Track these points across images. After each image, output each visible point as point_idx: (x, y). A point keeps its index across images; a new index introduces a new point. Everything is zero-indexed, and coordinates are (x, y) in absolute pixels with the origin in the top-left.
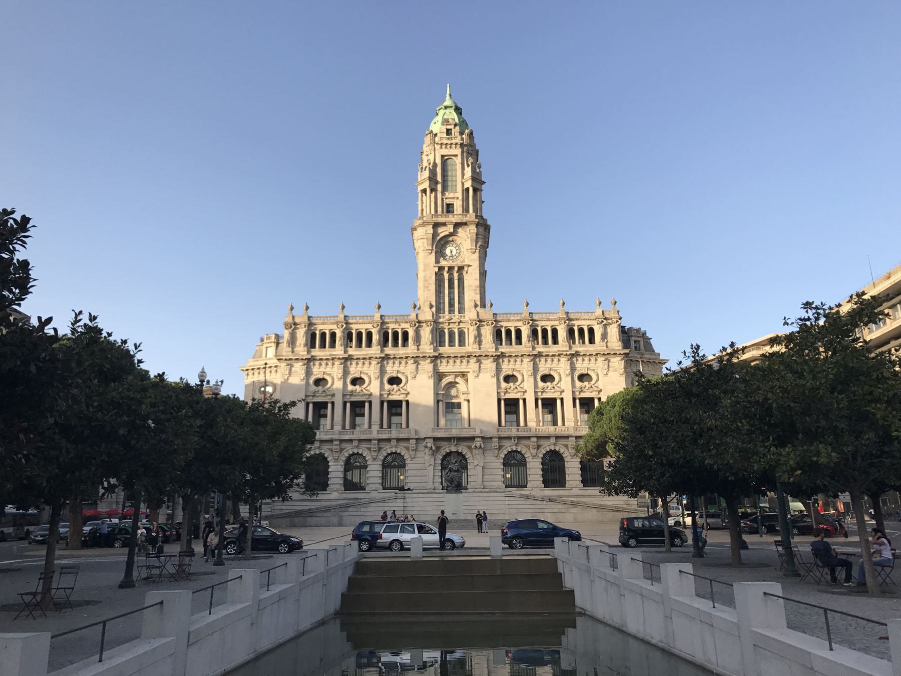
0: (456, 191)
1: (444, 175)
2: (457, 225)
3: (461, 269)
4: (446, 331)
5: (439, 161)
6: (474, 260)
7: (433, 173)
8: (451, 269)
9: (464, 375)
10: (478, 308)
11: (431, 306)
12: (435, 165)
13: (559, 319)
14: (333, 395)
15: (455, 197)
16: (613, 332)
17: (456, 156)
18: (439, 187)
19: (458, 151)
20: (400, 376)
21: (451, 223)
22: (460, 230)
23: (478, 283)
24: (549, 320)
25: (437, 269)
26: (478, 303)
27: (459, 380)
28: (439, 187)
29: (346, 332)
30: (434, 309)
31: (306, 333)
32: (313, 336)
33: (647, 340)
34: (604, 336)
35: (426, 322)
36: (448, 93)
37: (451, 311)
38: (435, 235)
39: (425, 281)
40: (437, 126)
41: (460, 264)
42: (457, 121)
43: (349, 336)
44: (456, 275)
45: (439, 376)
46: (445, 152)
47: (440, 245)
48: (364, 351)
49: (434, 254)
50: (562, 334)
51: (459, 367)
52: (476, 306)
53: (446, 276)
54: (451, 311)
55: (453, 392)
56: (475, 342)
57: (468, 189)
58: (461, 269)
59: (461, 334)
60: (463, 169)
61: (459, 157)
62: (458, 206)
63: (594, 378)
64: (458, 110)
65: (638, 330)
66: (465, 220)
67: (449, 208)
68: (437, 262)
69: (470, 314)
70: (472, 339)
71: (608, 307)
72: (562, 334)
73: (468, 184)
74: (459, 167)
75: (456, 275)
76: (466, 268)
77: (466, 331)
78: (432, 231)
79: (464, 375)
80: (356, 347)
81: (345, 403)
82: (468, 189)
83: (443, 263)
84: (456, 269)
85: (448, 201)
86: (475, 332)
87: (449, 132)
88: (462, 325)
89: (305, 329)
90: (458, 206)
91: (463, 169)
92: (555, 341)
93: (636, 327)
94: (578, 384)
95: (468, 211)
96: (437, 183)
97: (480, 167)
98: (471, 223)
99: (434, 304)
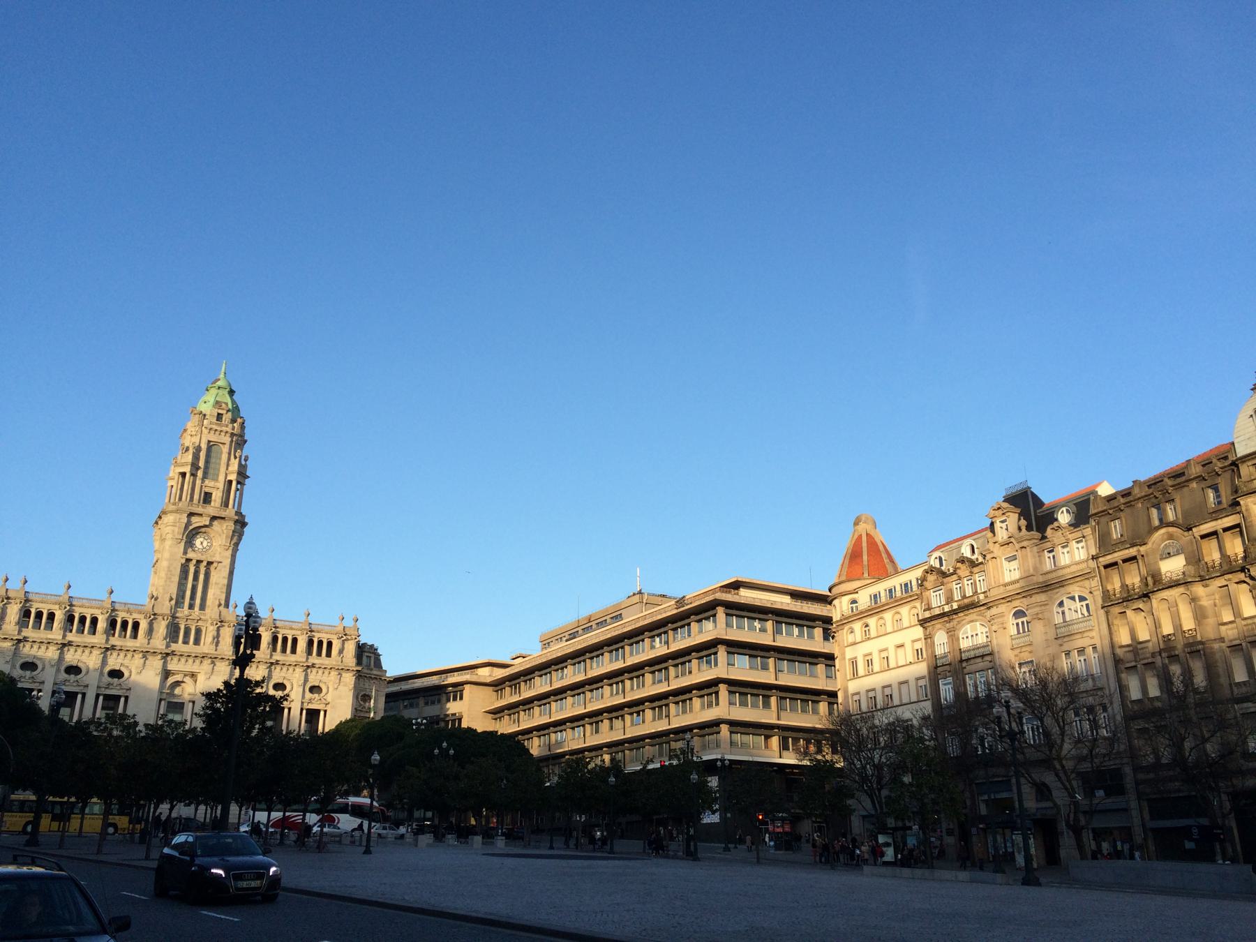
0: (216, 480)
1: (207, 462)
2: (214, 518)
3: (210, 563)
4: (182, 627)
5: (204, 446)
7: (196, 457)
8: (199, 562)
9: (193, 675)
10: (222, 608)
11: (171, 599)
12: (198, 449)
14: (43, 683)
15: (216, 488)
16: (351, 648)
18: (200, 473)
19: (227, 439)
20: (123, 669)
22: (215, 523)
23: (226, 581)
24: (291, 629)
27: (187, 679)
28: (200, 473)
30: (173, 602)
32: (27, 614)
33: (377, 656)
37: (191, 607)
38: (188, 524)
39: (169, 570)
40: (206, 405)
42: (230, 406)
43: (70, 619)
44: (203, 570)
45: (166, 674)
46: (213, 438)
47: (191, 535)
48: (87, 638)
49: (183, 544)
50: (302, 645)
51: (190, 666)
52: (220, 605)
53: (192, 569)
54: (191, 607)
55: (177, 691)
57: (230, 482)
58: (210, 563)
59: (198, 631)
60: (229, 459)
61: (227, 446)
62: (217, 496)
63: (324, 690)
64: (232, 392)
65: (372, 646)
66: (223, 514)
67: (207, 498)
68: (185, 553)
69: (212, 611)
70: (209, 639)
71: (348, 623)
72: (302, 645)
73: (233, 477)
74: (225, 457)
75: (203, 570)
77: (204, 630)
78: (185, 520)
79: (193, 675)
80: (78, 632)
81: (98, 696)
82: (230, 482)
83: (190, 555)
84: (205, 563)
85: (207, 490)
87: (219, 417)
88: (200, 623)
89: (20, 606)
90: (217, 496)
91: (229, 459)
92: (294, 651)
93: (370, 643)
94: (308, 695)
95: (227, 505)
96: (198, 468)
97: (246, 460)
98: (230, 519)
99: (174, 597)
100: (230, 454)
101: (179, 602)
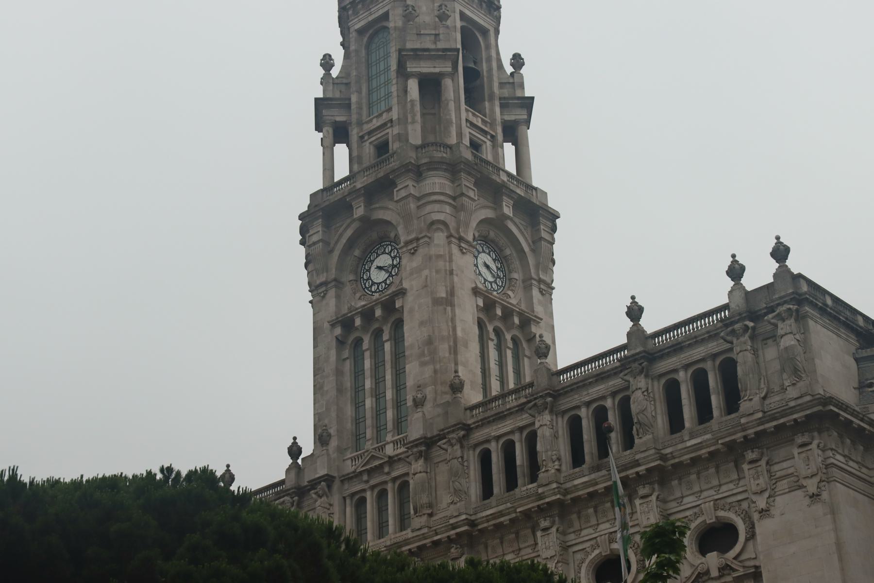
8: (367, 315)
25: (338, 331)
49: (332, 293)
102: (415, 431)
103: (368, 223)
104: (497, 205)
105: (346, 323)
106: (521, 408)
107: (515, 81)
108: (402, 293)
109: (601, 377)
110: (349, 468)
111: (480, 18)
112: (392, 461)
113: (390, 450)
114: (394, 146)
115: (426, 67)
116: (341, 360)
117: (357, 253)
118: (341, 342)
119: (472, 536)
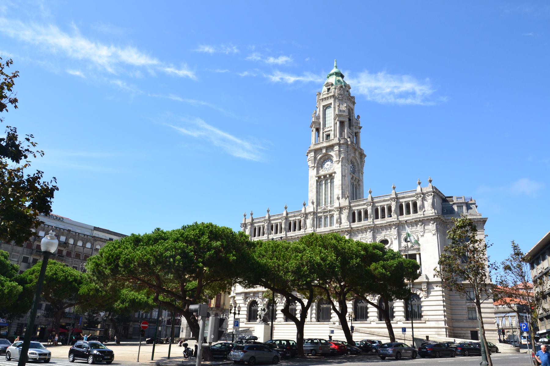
6: (339, 168)
8: (325, 176)
13: (391, 199)
17: (331, 104)
21: (324, 147)
24: (385, 201)
26: (340, 196)
29: (270, 225)
31: (251, 228)
34: (423, 206)
35: (310, 213)
36: (335, 65)
41: (330, 172)
49: (315, 169)
56: (337, 222)
58: (331, 175)
76: (333, 175)
86: (338, 216)
90: (332, 133)
99: (315, 201)
100: (334, 108)
101: (318, 204)
102: (336, 205)
103: (326, 154)
104: (355, 153)
105: (319, 177)
106: (364, 204)
107: (358, 123)
108: (335, 173)
109: (385, 201)
110: (319, 211)
111: (351, 106)
112: (330, 211)
113: (329, 208)
114: (332, 137)
115: (342, 119)
116: (317, 185)
117: (322, 160)
118: (317, 181)
119: (351, 232)
